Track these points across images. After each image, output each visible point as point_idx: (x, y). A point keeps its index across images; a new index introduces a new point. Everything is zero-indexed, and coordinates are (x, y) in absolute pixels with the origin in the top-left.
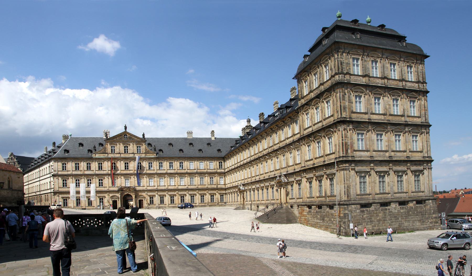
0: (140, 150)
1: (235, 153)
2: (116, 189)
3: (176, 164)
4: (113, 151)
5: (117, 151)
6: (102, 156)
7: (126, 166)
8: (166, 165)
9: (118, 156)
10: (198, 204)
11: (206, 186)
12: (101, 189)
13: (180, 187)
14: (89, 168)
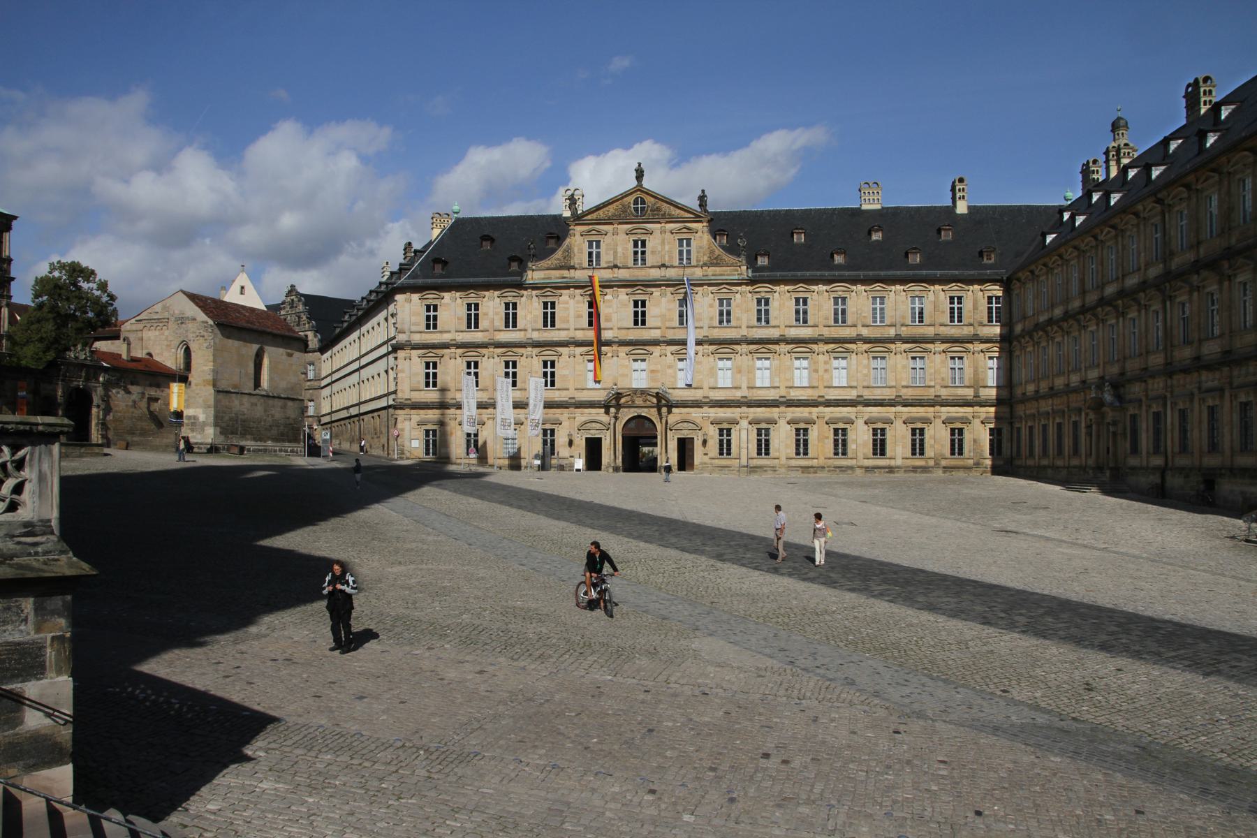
0: (689, 252)
2: (601, 396)
5: (606, 259)
6: (555, 276)
7: (636, 314)
10: (899, 462)
12: (556, 396)
13: (832, 395)
14: (511, 320)
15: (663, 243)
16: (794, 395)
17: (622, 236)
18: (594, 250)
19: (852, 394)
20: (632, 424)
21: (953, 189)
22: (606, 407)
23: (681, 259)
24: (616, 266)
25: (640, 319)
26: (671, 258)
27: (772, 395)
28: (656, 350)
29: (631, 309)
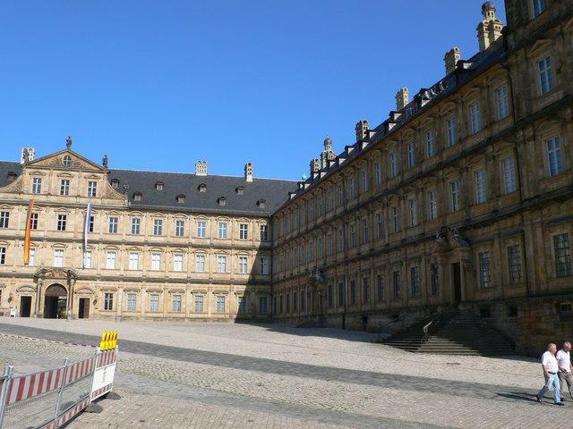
0: (94, 190)
1: (301, 202)
2: (33, 271)
3: (170, 223)
4: (36, 189)
6: (11, 197)
7: (60, 223)
8: (147, 221)
9: (43, 199)
10: (210, 316)
11: (228, 277)
13: (173, 276)
15: (79, 183)
16: (151, 275)
17: (54, 178)
18: (37, 184)
19: (184, 276)
20: (52, 289)
21: (245, 169)
22: (36, 278)
23: (89, 194)
24: (49, 194)
25: (62, 226)
26: (84, 192)
27: (138, 275)
28: (70, 245)
29: (57, 220)
